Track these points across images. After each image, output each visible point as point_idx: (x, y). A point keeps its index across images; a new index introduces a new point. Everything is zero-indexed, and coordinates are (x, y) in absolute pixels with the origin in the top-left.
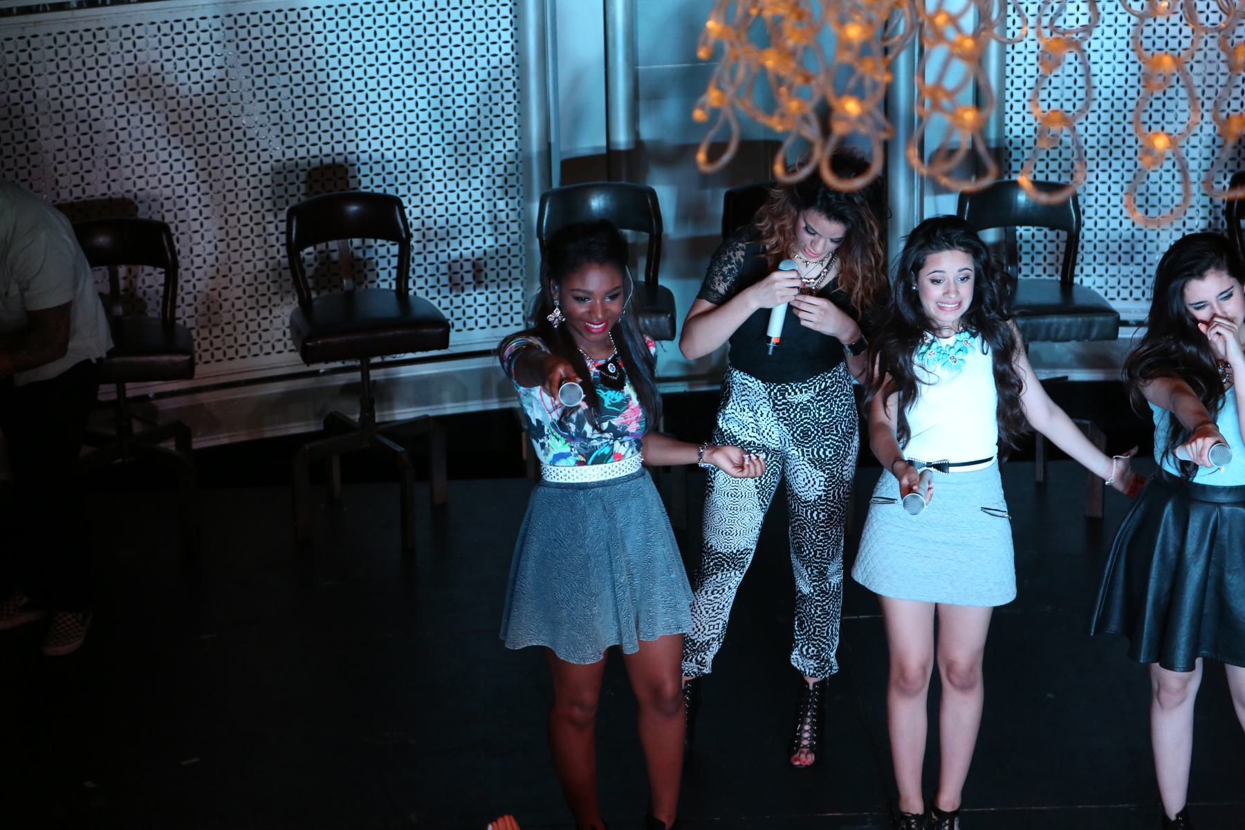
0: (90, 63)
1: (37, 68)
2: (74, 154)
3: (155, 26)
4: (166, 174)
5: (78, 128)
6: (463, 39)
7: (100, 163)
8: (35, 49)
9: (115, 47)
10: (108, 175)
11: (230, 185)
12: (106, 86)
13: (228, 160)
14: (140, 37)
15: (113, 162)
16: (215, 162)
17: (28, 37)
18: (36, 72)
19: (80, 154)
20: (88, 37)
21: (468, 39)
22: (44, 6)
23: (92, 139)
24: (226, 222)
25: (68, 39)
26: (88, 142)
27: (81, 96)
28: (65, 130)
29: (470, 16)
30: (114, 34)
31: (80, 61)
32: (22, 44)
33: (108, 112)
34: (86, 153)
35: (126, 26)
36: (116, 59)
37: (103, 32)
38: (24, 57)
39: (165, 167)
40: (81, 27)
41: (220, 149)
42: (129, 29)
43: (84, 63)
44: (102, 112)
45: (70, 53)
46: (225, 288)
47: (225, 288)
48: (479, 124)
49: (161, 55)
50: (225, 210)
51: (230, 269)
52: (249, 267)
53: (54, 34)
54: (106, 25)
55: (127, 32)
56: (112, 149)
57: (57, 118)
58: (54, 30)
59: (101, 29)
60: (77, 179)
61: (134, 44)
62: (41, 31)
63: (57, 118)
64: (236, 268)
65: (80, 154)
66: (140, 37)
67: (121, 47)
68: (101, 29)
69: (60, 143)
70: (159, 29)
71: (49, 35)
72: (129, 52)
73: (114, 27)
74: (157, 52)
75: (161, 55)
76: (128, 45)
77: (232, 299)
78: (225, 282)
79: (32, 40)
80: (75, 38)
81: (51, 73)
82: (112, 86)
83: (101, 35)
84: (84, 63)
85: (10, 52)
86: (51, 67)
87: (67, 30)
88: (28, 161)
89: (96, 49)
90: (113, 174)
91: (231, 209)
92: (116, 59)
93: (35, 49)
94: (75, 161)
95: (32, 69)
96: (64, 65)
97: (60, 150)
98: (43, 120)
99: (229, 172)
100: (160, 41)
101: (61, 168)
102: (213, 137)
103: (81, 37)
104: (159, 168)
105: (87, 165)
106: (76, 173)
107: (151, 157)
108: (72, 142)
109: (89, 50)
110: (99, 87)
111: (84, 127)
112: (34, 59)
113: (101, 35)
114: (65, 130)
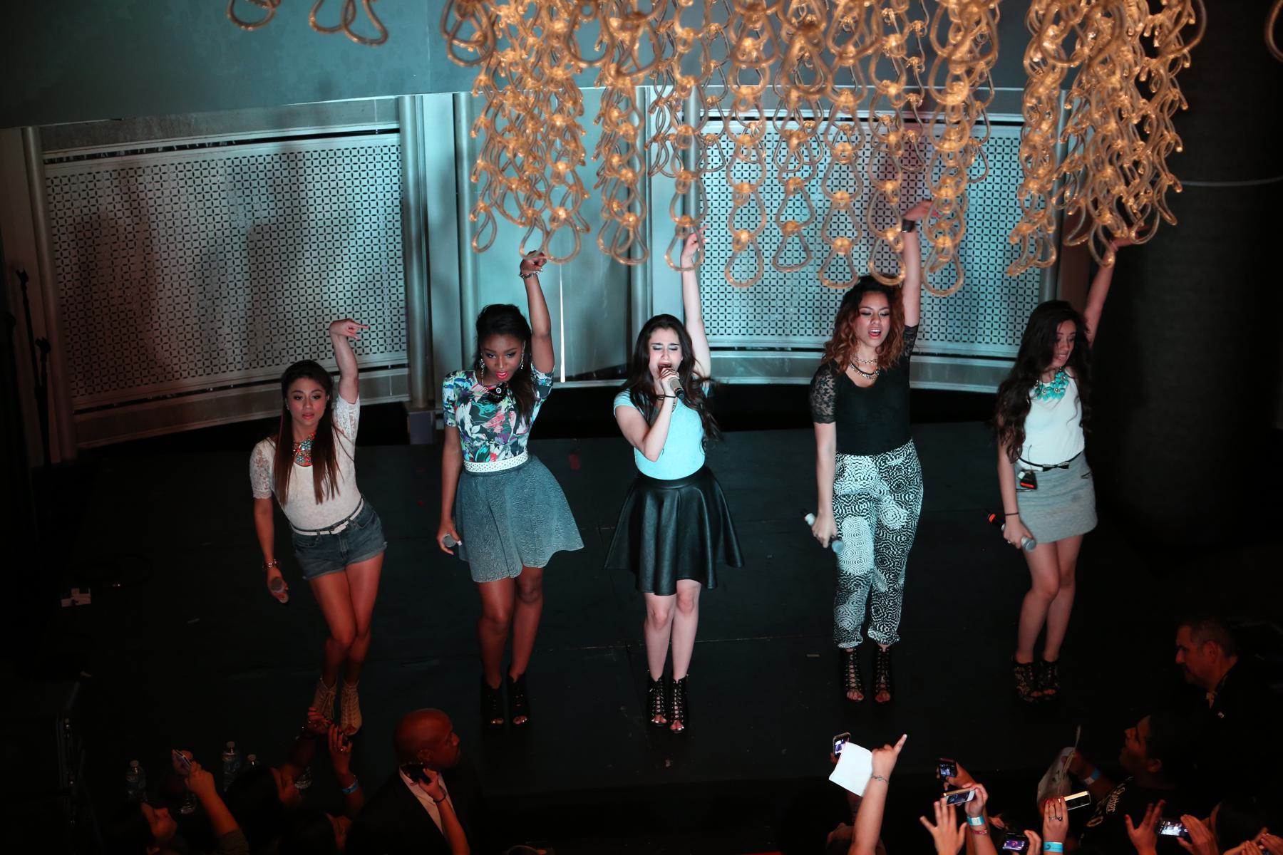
1: (100, 193)
2: (124, 245)
3: (174, 166)
4: (181, 257)
6: (368, 174)
8: (98, 181)
9: (149, 179)
10: (145, 258)
11: (222, 264)
14: (164, 173)
17: (94, 173)
18: (99, 194)
19: (127, 245)
21: (371, 174)
22: (104, 154)
24: (220, 287)
26: (132, 238)
29: (372, 160)
32: (90, 177)
34: (131, 245)
35: (155, 166)
36: (150, 186)
38: (91, 185)
39: (181, 254)
41: (216, 241)
42: (158, 168)
43: (129, 189)
46: (220, 328)
47: (220, 328)
48: (378, 226)
50: (219, 279)
51: (223, 316)
52: (234, 315)
54: (143, 166)
55: (156, 170)
61: (161, 177)
62: (102, 169)
65: (127, 245)
66: (164, 173)
69: (114, 239)
72: (158, 182)
78: (220, 324)
79: (96, 175)
81: (108, 196)
84: (129, 189)
85: (83, 182)
86: (109, 191)
91: (223, 279)
92: (150, 186)
93: (98, 181)
94: (124, 249)
95: (96, 193)
100: (177, 176)
101: (115, 254)
102: (211, 235)
105: (132, 252)
107: (172, 247)
112: (97, 186)
113: (140, 172)
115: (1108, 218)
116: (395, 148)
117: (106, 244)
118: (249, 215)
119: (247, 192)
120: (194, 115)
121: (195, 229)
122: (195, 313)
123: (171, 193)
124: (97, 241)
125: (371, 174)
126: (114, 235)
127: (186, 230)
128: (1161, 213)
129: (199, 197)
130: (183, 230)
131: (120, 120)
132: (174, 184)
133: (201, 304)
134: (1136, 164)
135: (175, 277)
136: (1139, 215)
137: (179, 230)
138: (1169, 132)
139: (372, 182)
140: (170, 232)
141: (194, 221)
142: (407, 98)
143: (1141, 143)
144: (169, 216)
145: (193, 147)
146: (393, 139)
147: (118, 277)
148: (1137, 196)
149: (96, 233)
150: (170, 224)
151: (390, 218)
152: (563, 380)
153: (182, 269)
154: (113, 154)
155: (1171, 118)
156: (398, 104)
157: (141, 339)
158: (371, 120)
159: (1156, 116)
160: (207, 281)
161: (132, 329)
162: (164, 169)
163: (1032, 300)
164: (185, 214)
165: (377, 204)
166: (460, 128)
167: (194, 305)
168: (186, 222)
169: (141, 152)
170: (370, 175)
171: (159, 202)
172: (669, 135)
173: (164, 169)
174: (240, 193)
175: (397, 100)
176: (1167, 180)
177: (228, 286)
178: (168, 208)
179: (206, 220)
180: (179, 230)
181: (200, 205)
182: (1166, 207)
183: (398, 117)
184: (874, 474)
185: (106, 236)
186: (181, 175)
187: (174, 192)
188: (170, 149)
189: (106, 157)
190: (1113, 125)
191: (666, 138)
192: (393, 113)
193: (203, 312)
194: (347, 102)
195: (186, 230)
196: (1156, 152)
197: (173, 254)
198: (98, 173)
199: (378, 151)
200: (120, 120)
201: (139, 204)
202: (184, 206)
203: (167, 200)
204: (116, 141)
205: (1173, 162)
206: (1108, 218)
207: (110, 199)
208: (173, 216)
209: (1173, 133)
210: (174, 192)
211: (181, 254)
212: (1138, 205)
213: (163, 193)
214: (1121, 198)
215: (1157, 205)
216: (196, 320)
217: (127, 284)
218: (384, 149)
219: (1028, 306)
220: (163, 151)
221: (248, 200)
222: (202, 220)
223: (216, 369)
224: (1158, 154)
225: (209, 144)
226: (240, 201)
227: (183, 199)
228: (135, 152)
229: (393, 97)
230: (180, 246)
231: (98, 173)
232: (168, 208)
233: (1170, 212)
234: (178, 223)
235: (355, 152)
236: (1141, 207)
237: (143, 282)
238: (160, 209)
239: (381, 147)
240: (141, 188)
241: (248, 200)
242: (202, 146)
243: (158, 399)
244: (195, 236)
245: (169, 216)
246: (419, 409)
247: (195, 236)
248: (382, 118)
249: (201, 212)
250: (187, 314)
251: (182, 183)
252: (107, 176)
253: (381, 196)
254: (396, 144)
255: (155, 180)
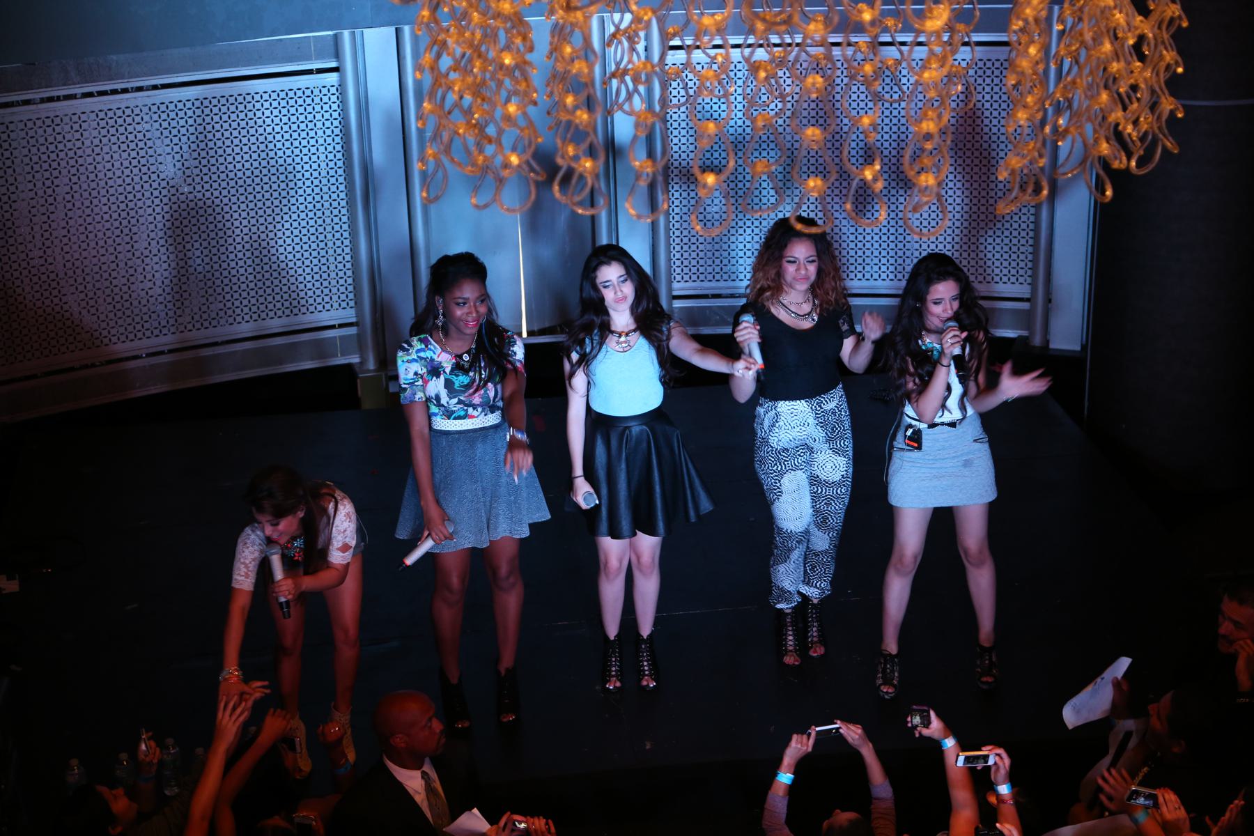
0: (51, 139)
1: (14, 144)
2: (42, 201)
5: (44, 184)
7: (60, 207)
8: (12, 131)
9: (67, 128)
10: (66, 215)
11: (151, 219)
12: (62, 155)
13: (149, 202)
14: (84, 121)
15: (69, 206)
16: (140, 204)
20: (48, 122)
21: (310, 117)
22: (18, 102)
23: (54, 191)
25: (35, 124)
27: (45, 162)
28: (35, 185)
30: (66, 119)
31: (43, 138)
33: (64, 172)
34: (51, 200)
35: (74, 114)
36: (68, 137)
37: (58, 119)
39: (105, 209)
40: (43, 115)
43: (46, 140)
44: (60, 172)
45: (36, 132)
46: (151, 289)
47: (151, 289)
49: (100, 133)
50: (148, 236)
51: (154, 276)
53: (25, 121)
54: (60, 114)
55: (75, 118)
56: (68, 197)
57: (29, 177)
58: (25, 118)
59: (57, 116)
60: (45, 218)
62: (16, 118)
63: (29, 177)
64: (157, 275)
66: (84, 121)
67: (72, 128)
68: (57, 116)
69: (32, 194)
70: (97, 116)
71: (22, 121)
73: (66, 115)
74: (97, 131)
75: (100, 133)
76: (76, 127)
77: (156, 296)
78: (150, 285)
80: (39, 123)
82: (67, 155)
83: (57, 121)
84: (46, 140)
86: (24, 143)
87: (34, 117)
88: (11, 207)
89: (54, 130)
90: (70, 214)
91: (152, 235)
92: (68, 137)
93: (12, 131)
96: (33, 141)
97: (32, 199)
98: (20, 179)
99: (150, 211)
100: (98, 124)
102: (138, 187)
103: (44, 122)
104: (101, 209)
105: (52, 208)
106: (44, 214)
107: (95, 202)
108: (40, 193)
109: (49, 130)
110: (58, 156)
111: (48, 183)
114: (35, 185)
115: (1104, 148)
116: (335, 88)
117: (23, 200)
118: (179, 165)
119: (176, 140)
120: (115, 57)
121: (120, 181)
122: (123, 273)
123: (92, 143)
124: (13, 197)
125: (310, 117)
126: (31, 190)
127: (110, 183)
128: (1162, 140)
129: (124, 147)
130: (106, 183)
131: (34, 64)
132: (95, 133)
133: (130, 264)
134: (1134, 88)
135: (100, 235)
136: (1139, 144)
137: (102, 183)
138: (1167, 51)
139: (311, 125)
140: (93, 185)
141: (118, 173)
142: (346, 34)
143: (1138, 64)
144: (91, 168)
145: (114, 92)
146: (333, 78)
147: (38, 236)
148: (1136, 123)
149: (12, 189)
150: (92, 177)
151: (331, 164)
152: (525, 335)
153: (108, 225)
154: (27, 102)
155: (1173, 37)
156: (337, 39)
157: (65, 303)
158: (308, 58)
159: (1154, 35)
160: (135, 238)
161: (55, 292)
162: (83, 117)
163: (1028, 234)
164: (109, 166)
165: (318, 150)
166: (405, 65)
167: (122, 265)
168: (110, 174)
169: (58, 99)
170: (309, 119)
171: (79, 152)
172: (628, 70)
173: (83, 117)
174: (167, 141)
175: (336, 35)
176: (1168, 104)
177: (158, 243)
178: (90, 160)
179: (132, 172)
180: (102, 183)
181: (125, 155)
182: (1166, 131)
183: (337, 55)
184: (811, 420)
185: (23, 191)
186: (103, 123)
187: (96, 142)
188: (90, 95)
189: (19, 105)
190: (1107, 47)
191: (625, 72)
192: (332, 49)
193: (131, 271)
194: (281, 40)
195: (110, 183)
196: (1154, 75)
197: (96, 210)
198: (11, 122)
199: (316, 92)
200: (34, 64)
201: (58, 156)
202: (107, 157)
203: (89, 151)
204: (28, 87)
205: (1174, 85)
206: (1104, 148)
207: (25, 151)
208: (95, 168)
209: (1174, 53)
210: (96, 142)
211: (105, 209)
212: (1139, 132)
213: (83, 143)
214: (1117, 125)
215: (1157, 131)
216: (124, 281)
217: (48, 243)
218: (323, 89)
219: (908, 261)
220: (81, 98)
221: (177, 149)
222: (127, 172)
223: (148, 333)
224: (1157, 75)
225: (132, 88)
226: (168, 150)
227: (106, 149)
228: (51, 99)
229: (330, 33)
230: (104, 200)
231: (11, 122)
232: (90, 160)
233: (1170, 138)
234: (101, 175)
235: (291, 94)
236: (1141, 134)
237: (65, 240)
238: (81, 161)
239: (320, 87)
240: (59, 138)
241: (177, 149)
242: (125, 91)
243: (86, 367)
244: (121, 190)
245: (91, 168)
246: (369, 371)
247: (121, 190)
248: (320, 56)
249: (126, 164)
250: (114, 274)
251: (104, 132)
252: (21, 126)
253: (321, 141)
254: (336, 85)
255: (75, 129)
